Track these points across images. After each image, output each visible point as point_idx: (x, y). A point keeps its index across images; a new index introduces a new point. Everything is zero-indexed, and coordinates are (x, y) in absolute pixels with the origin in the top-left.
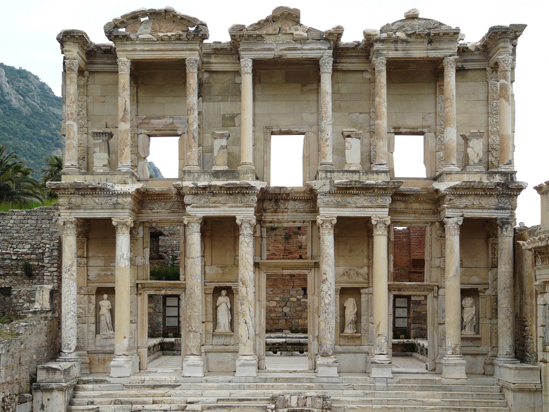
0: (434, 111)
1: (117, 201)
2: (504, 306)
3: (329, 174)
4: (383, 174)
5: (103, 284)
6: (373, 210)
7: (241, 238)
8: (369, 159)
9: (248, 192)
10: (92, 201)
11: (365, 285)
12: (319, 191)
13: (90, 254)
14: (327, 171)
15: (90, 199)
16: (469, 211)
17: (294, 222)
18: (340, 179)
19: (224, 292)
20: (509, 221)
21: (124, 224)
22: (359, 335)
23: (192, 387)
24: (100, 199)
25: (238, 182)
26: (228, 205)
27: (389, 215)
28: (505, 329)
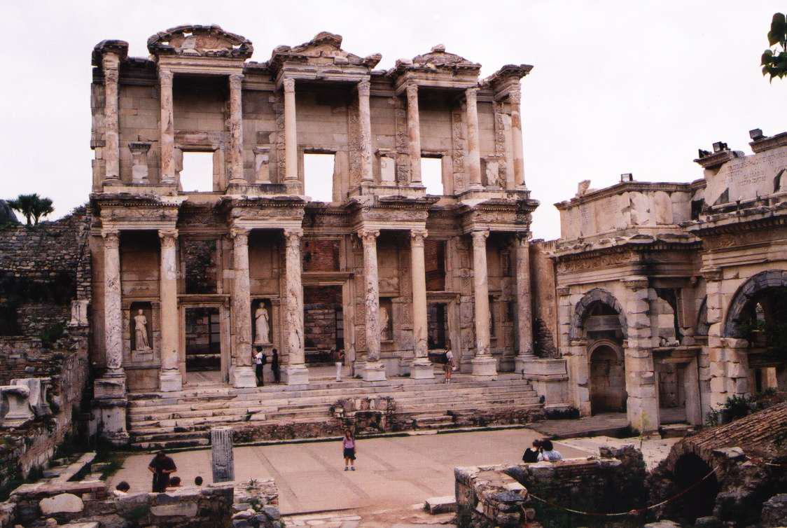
0: (450, 137)
1: (163, 213)
2: (524, 309)
3: (371, 190)
4: (420, 191)
6: (412, 223)
7: (289, 251)
8: (401, 175)
11: (395, 295)
12: (364, 205)
13: (124, 268)
14: (369, 187)
16: (494, 225)
17: (329, 235)
18: (385, 194)
19: (262, 305)
20: (524, 235)
21: (171, 236)
22: (392, 341)
23: (249, 398)
24: (146, 211)
25: (288, 196)
27: (426, 228)
28: (526, 329)
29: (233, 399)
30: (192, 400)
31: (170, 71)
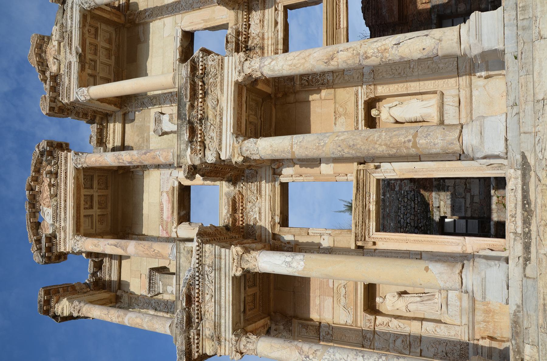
5: (359, 301)
9: (201, 68)
10: (209, 305)
15: (207, 307)
17: (276, 23)
23: (528, 127)
24: (207, 292)
26: (219, 95)
29: (531, 161)
30: (527, 247)
31: (72, 239)
